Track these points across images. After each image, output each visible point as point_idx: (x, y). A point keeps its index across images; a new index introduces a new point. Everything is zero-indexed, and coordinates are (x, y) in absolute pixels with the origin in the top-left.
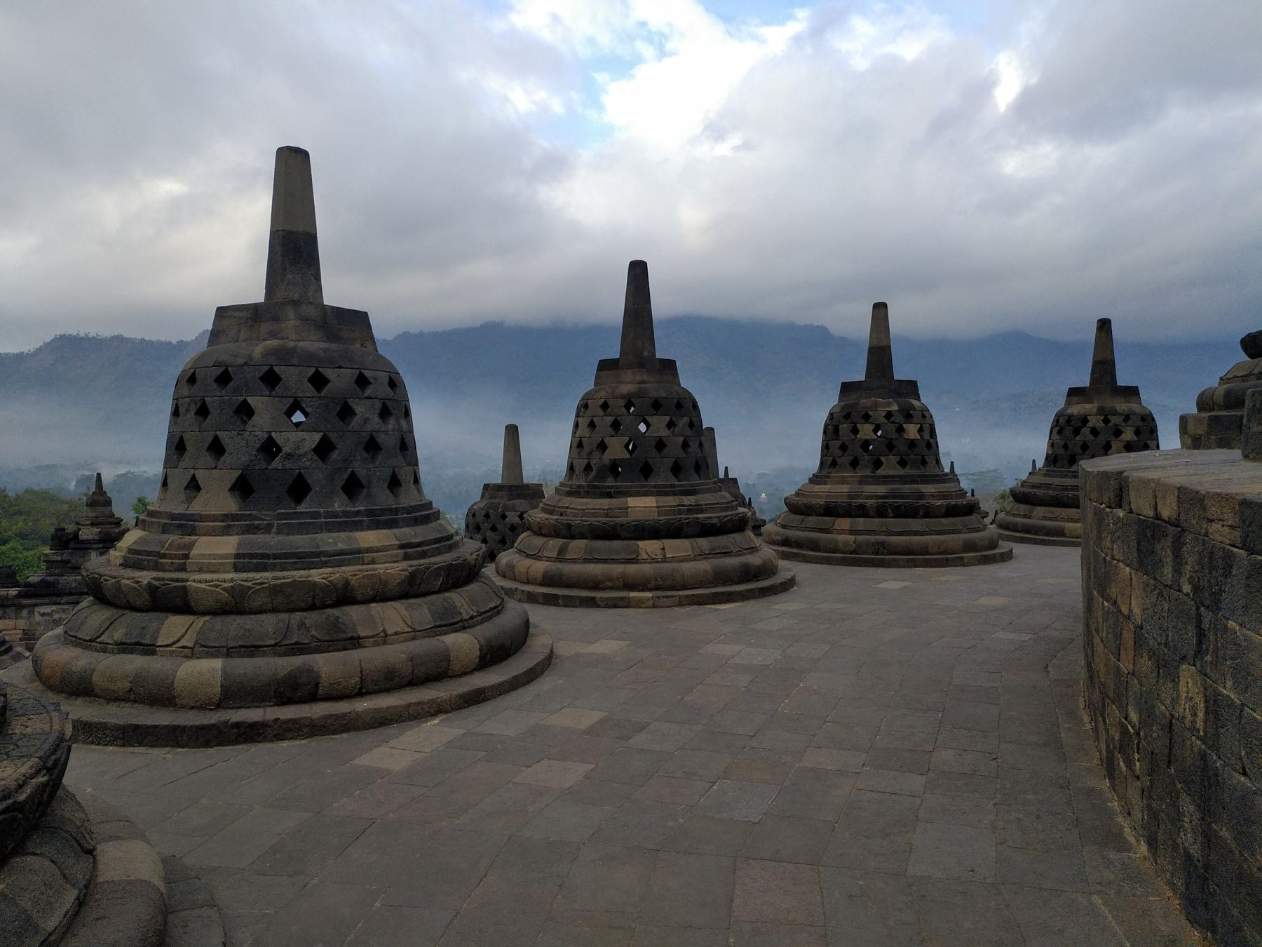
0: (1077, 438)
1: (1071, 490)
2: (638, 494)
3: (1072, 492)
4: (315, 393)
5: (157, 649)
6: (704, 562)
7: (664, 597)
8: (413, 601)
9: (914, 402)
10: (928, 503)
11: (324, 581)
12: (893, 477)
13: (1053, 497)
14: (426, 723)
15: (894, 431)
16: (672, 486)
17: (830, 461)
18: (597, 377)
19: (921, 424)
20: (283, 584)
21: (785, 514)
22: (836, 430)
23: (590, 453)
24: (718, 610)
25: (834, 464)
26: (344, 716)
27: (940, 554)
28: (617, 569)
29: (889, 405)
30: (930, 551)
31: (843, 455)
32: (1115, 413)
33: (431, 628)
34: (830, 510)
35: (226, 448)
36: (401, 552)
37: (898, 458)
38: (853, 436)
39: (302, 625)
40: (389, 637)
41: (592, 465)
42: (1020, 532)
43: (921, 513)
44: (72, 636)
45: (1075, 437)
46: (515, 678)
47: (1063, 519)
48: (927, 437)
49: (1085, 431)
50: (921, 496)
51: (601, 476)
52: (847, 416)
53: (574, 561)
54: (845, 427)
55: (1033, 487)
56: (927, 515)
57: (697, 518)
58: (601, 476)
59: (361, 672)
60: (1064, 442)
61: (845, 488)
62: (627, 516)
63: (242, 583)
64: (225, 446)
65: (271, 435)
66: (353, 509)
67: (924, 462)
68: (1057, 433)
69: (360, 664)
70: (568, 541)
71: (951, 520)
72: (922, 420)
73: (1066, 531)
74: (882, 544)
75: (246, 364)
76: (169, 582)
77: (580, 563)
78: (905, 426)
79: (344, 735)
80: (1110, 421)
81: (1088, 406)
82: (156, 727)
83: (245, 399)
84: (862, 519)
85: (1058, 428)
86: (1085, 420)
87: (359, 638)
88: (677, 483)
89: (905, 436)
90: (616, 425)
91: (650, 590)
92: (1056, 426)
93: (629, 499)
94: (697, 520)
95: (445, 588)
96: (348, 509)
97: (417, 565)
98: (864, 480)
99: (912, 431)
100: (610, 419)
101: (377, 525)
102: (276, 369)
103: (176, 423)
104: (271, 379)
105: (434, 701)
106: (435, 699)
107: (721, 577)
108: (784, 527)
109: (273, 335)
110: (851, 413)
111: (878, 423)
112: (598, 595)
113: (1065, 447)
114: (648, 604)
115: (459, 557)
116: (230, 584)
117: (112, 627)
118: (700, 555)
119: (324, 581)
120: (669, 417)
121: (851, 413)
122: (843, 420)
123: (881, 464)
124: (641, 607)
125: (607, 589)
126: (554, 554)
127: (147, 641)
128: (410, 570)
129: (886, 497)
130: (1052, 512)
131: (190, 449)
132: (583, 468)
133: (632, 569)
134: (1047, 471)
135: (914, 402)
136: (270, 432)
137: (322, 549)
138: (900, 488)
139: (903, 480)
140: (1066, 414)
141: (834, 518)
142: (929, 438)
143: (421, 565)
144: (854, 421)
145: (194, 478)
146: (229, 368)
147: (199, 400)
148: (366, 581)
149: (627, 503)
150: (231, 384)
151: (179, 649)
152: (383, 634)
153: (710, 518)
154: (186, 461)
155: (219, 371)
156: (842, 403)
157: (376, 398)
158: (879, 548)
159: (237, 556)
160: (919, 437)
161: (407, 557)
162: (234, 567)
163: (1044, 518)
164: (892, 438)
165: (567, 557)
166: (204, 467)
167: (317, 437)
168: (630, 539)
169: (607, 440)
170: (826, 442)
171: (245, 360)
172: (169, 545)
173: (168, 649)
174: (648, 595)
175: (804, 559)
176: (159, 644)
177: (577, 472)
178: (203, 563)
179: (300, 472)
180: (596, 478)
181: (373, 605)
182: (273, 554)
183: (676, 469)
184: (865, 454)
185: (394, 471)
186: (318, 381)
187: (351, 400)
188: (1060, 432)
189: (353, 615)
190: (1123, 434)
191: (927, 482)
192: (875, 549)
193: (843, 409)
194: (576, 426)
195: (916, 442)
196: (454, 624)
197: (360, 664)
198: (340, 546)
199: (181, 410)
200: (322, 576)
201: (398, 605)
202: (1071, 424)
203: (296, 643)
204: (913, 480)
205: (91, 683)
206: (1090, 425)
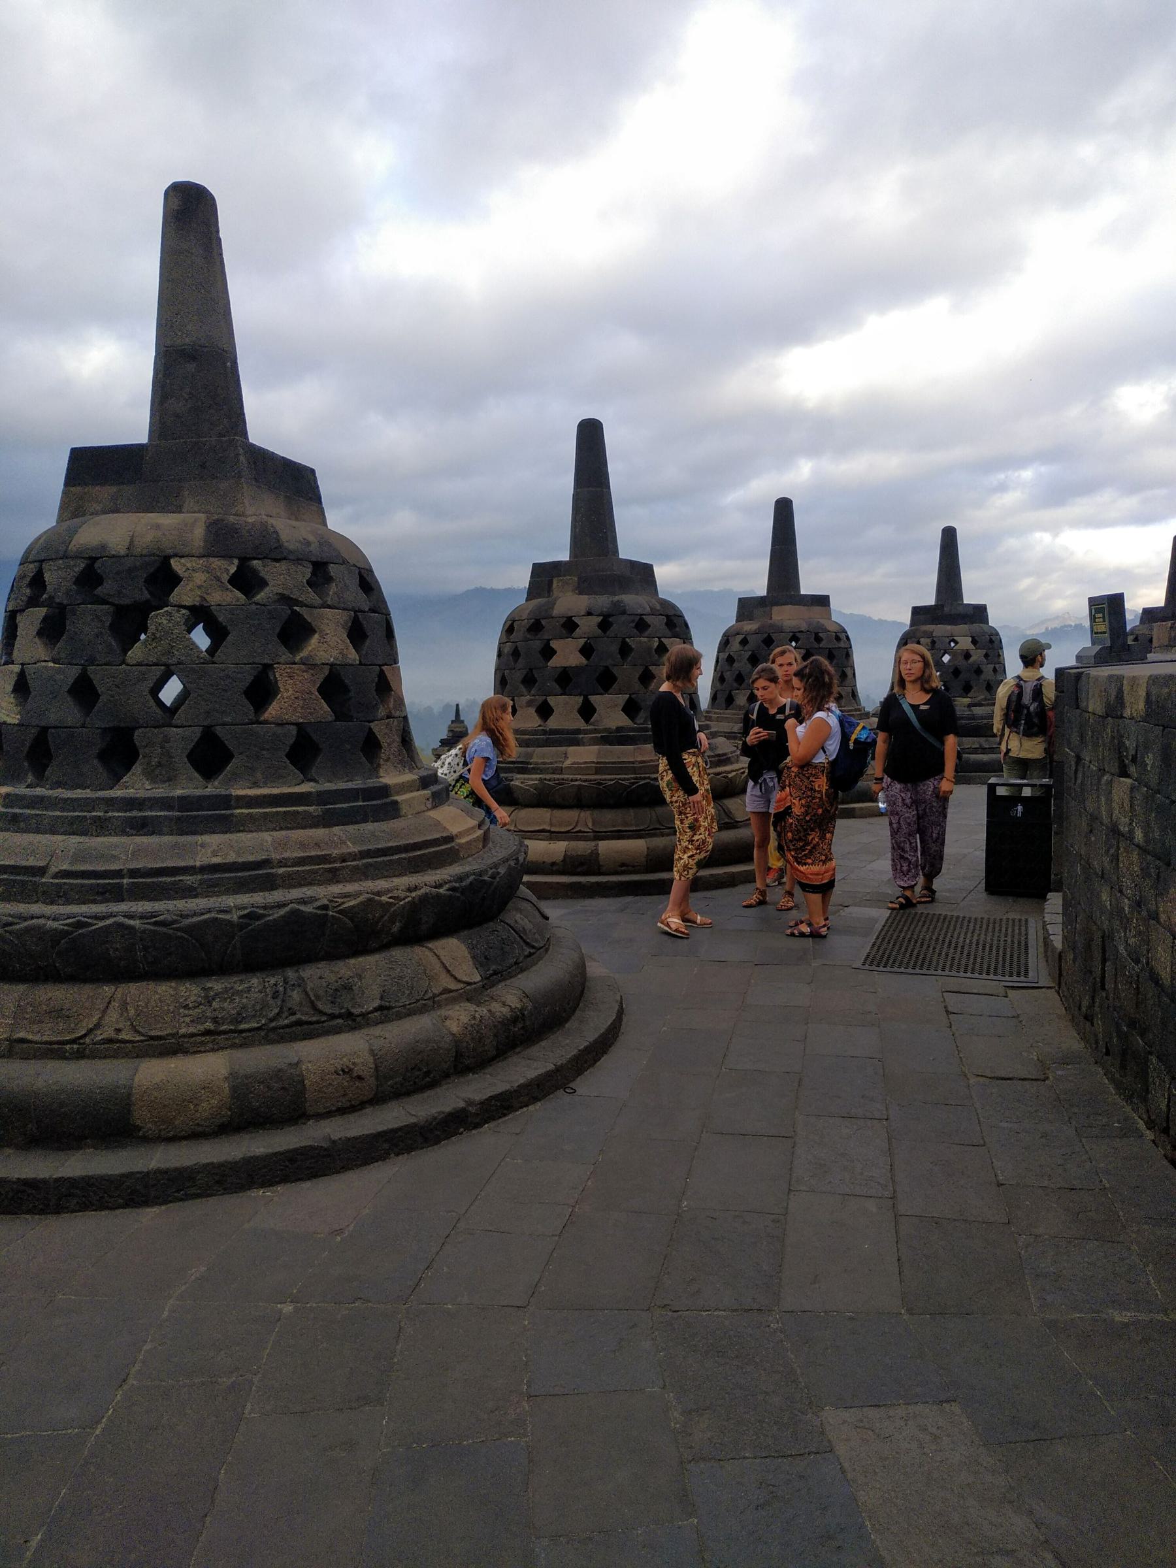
0: (136, 653)
1: (138, 893)
13: (57, 936)
32: (276, 553)
45: (125, 651)
47: (114, 1049)
60: (74, 672)
73: (141, 1116)
80: (263, 583)
81: (168, 520)
85: (44, 610)
92: (33, 602)
130: (57, 1013)
140: (72, 547)
188: (52, 630)
190: (314, 640)
202: (99, 591)
206: (184, 594)
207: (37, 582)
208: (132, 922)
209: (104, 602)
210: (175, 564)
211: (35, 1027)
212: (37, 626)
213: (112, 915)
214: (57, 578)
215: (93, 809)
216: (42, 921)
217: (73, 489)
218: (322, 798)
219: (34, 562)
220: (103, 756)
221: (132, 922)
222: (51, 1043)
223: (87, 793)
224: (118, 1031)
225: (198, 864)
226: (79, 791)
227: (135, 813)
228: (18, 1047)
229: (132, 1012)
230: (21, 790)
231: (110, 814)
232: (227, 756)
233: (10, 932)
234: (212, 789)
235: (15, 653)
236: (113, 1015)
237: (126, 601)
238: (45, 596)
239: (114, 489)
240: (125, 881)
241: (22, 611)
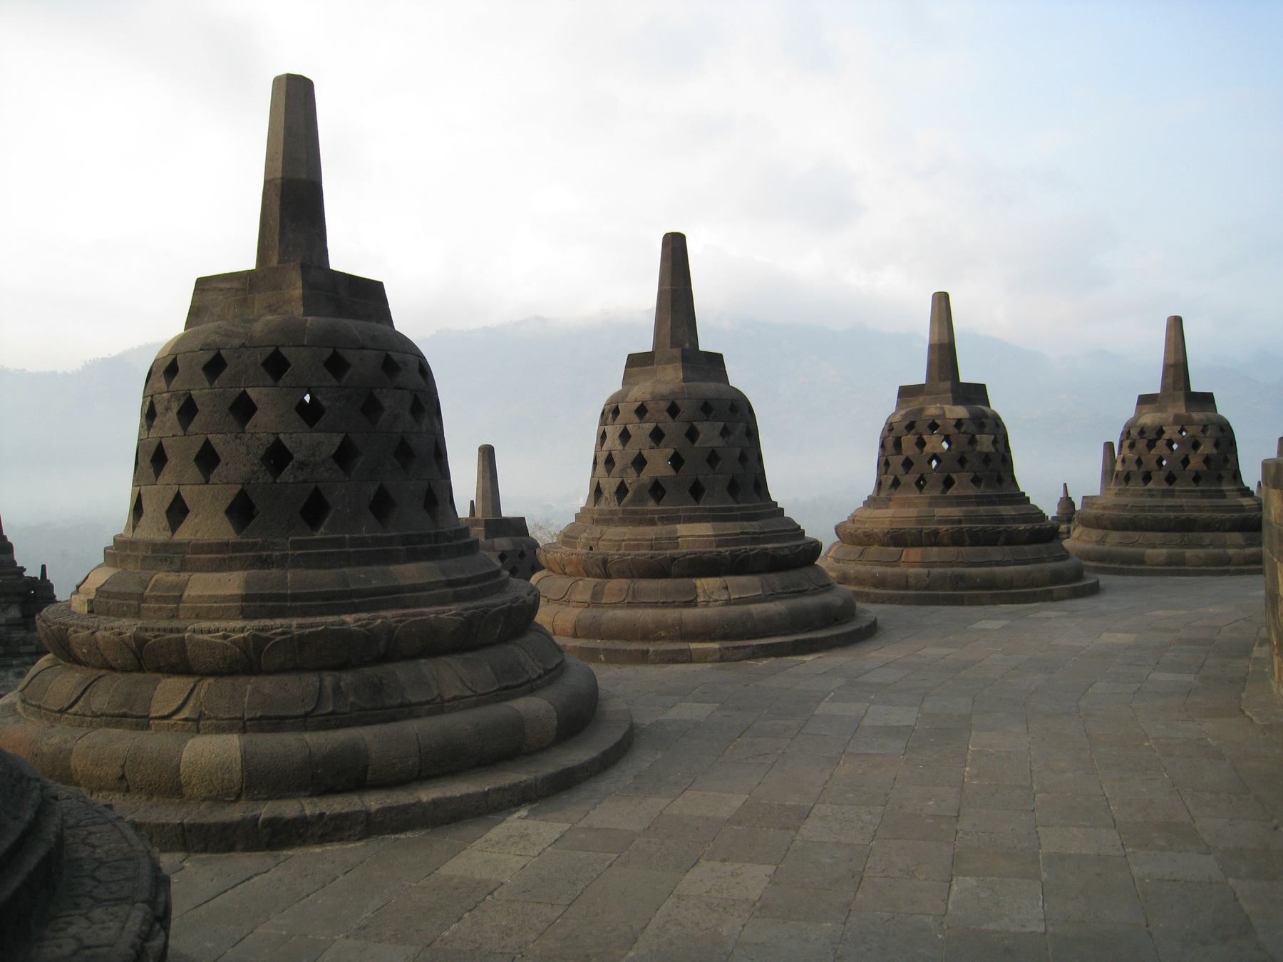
0: (1153, 451)
2: (690, 520)
3: (1151, 514)
4: (334, 382)
5: (151, 722)
6: (778, 603)
7: (734, 648)
8: (468, 655)
10: (1009, 528)
11: (363, 629)
12: (971, 497)
14: (512, 813)
16: (731, 509)
17: (890, 481)
18: (627, 375)
20: (310, 633)
21: (835, 547)
22: (898, 444)
23: (624, 470)
24: (805, 662)
25: (896, 483)
26: (405, 809)
27: (1026, 587)
28: (672, 614)
31: (907, 473)
33: (495, 691)
34: (898, 539)
35: (220, 456)
36: (450, 590)
37: (971, 475)
39: (337, 689)
40: (447, 704)
41: (628, 485)
43: (1002, 539)
44: (35, 706)
46: (604, 754)
47: (1142, 545)
49: (1161, 443)
50: (1000, 519)
51: (638, 499)
52: (911, 426)
53: (614, 606)
54: (908, 441)
56: (1009, 542)
57: (767, 549)
58: (638, 499)
59: (420, 752)
60: (1136, 457)
61: (912, 512)
62: (677, 546)
63: (261, 634)
64: (219, 453)
65: (278, 437)
66: (385, 535)
67: (1000, 480)
68: (1129, 447)
69: (418, 737)
70: (605, 580)
71: (1034, 547)
74: (961, 578)
75: (243, 345)
76: (162, 634)
77: (622, 608)
78: (978, 436)
79: (409, 835)
82: (163, 825)
83: (245, 392)
84: (935, 549)
86: (1160, 432)
87: (410, 705)
88: (736, 506)
89: (978, 448)
90: (657, 435)
91: (712, 640)
92: (1127, 438)
93: (678, 526)
94: (764, 553)
95: (504, 639)
96: (379, 534)
97: (473, 608)
98: (933, 502)
99: (985, 442)
100: (649, 427)
101: (414, 556)
102: (283, 351)
103: (149, 427)
104: (276, 365)
105: (516, 786)
106: (515, 785)
107: (797, 622)
108: (838, 561)
109: (271, 309)
111: (947, 433)
112: (652, 647)
113: (1139, 462)
114: (714, 658)
115: (517, 599)
116: (242, 635)
117: (87, 693)
118: (772, 594)
119: (363, 629)
120: (723, 424)
124: (705, 662)
125: (659, 639)
126: (587, 597)
127: (138, 711)
128: (466, 614)
129: (960, 522)
131: (172, 460)
132: (614, 489)
133: (688, 614)
136: (277, 434)
137: (353, 588)
139: (980, 500)
140: (1138, 424)
141: (901, 549)
142: (1004, 451)
143: (477, 608)
144: (920, 431)
145: (178, 495)
146: (223, 352)
147: (184, 395)
148: (414, 630)
149: (675, 532)
150: (227, 370)
151: (180, 722)
152: (439, 700)
153: (780, 548)
154: (167, 475)
155: (207, 357)
156: (903, 412)
157: (407, 389)
159: (246, 598)
160: (993, 450)
161: (458, 598)
162: (242, 613)
165: (604, 601)
166: (192, 482)
167: (337, 439)
168: (682, 576)
169: (645, 453)
170: (884, 458)
171: (243, 341)
172: (154, 586)
173: (166, 722)
174: (715, 645)
176: (153, 715)
177: (606, 494)
178: (201, 607)
179: (316, 486)
180: (633, 502)
181: (423, 661)
182: (293, 595)
183: (733, 488)
185: (429, 485)
186: (336, 365)
187: (379, 390)
189: (401, 672)
193: (905, 417)
194: (603, 437)
196: (520, 685)
197: (418, 740)
198: (375, 583)
199: (159, 409)
200: (359, 623)
201: (453, 660)
202: (1144, 436)
203: (332, 713)
204: (989, 501)
205: (69, 767)
206: (1166, 436)
207: (1129, 433)
210: (1164, 428)
214: (1134, 433)
218: (1202, 491)
225: (1165, 504)
232: (1175, 479)
234: (1171, 487)
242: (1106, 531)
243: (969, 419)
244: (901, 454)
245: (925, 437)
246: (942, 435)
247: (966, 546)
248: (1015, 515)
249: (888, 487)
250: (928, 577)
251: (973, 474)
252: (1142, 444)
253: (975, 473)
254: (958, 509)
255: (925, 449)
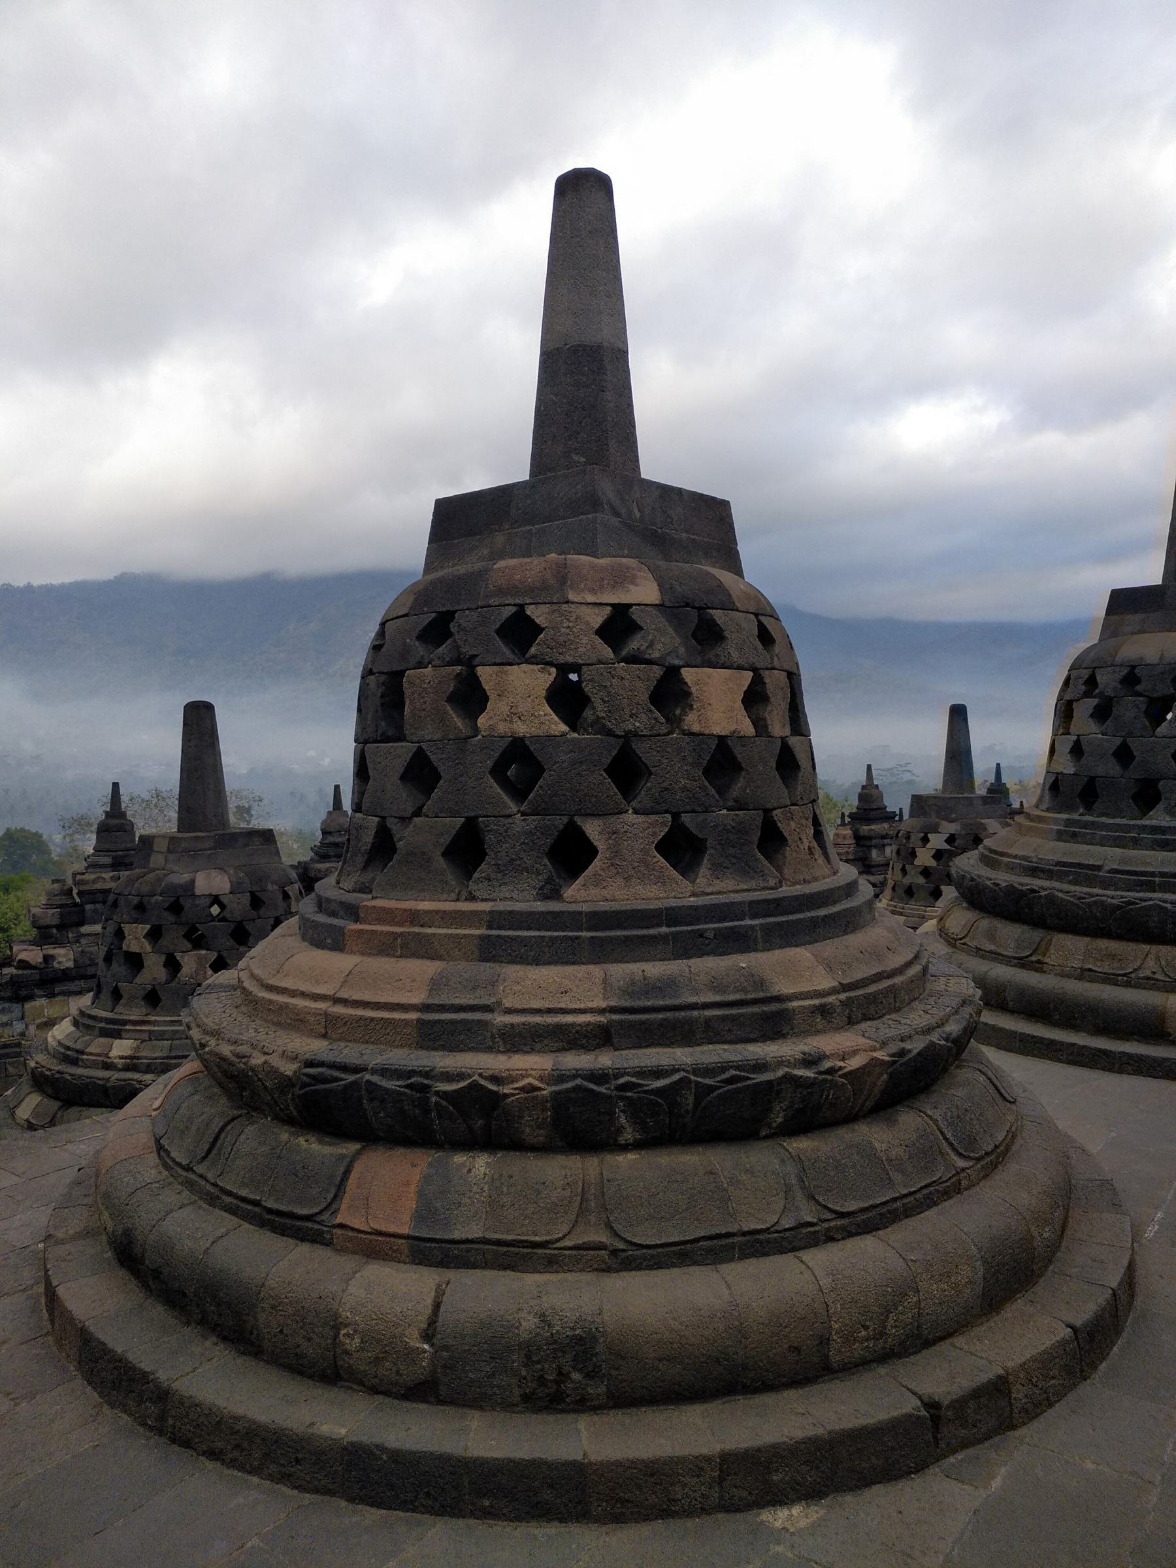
0: (1162, 729)
9: (725, 577)
10: (809, 1061)
15: (644, 697)
19: (754, 670)
29: (620, 579)
30: (835, 1358)
31: (418, 813)
37: (661, 825)
38: (458, 722)
42: (1012, 1012)
47: (1150, 983)
48: (779, 727)
55: (1034, 871)
60: (1118, 741)
72: (760, 657)
78: (688, 674)
84: (481, 1164)
92: (1087, 695)
110: (447, 617)
113: (1124, 755)
121: (447, 617)
122: (420, 649)
123: (591, 852)
129: (603, 1037)
130: (1112, 956)
134: (1068, 823)
135: (725, 577)
138: (669, 985)
140: (1118, 660)
141: (354, 1147)
142: (787, 731)
144: (469, 651)
156: (430, 577)
158: (562, 1375)
160: (747, 728)
163: (1084, 974)
164: (636, 735)
175: (162, 1418)
184: (513, 808)
188: (1102, 713)
191: (787, 936)
192: (541, 1381)
195: (738, 751)
202: (1138, 688)
207: (1091, 682)
208: (1165, 905)
209: (1140, 695)
211: (1099, 963)
212: (1091, 711)
213: (1151, 899)
214: (1107, 680)
215: (1129, 832)
216: (1105, 898)
217: (1112, 618)
219: (1086, 668)
220: (1135, 798)
221: (1165, 905)
222: (1110, 974)
223: (1124, 821)
224: (1154, 973)
226: (1119, 819)
227: (1159, 836)
228: (1087, 973)
229: (1163, 963)
230: (1076, 816)
231: (1142, 836)
233: (1082, 903)
235: (1073, 729)
236: (1151, 963)
237: (1155, 695)
238: (1097, 691)
239: (1144, 616)
240: (1157, 879)
241: (1077, 700)
242: (1037, 935)
243: (659, 606)
244: (401, 738)
245: (484, 673)
246: (551, 664)
247: (625, 1148)
248: (834, 991)
249: (360, 860)
250: (427, 1336)
251: (669, 817)
252: (1130, 710)
253: (676, 816)
254: (596, 970)
255: (482, 721)
